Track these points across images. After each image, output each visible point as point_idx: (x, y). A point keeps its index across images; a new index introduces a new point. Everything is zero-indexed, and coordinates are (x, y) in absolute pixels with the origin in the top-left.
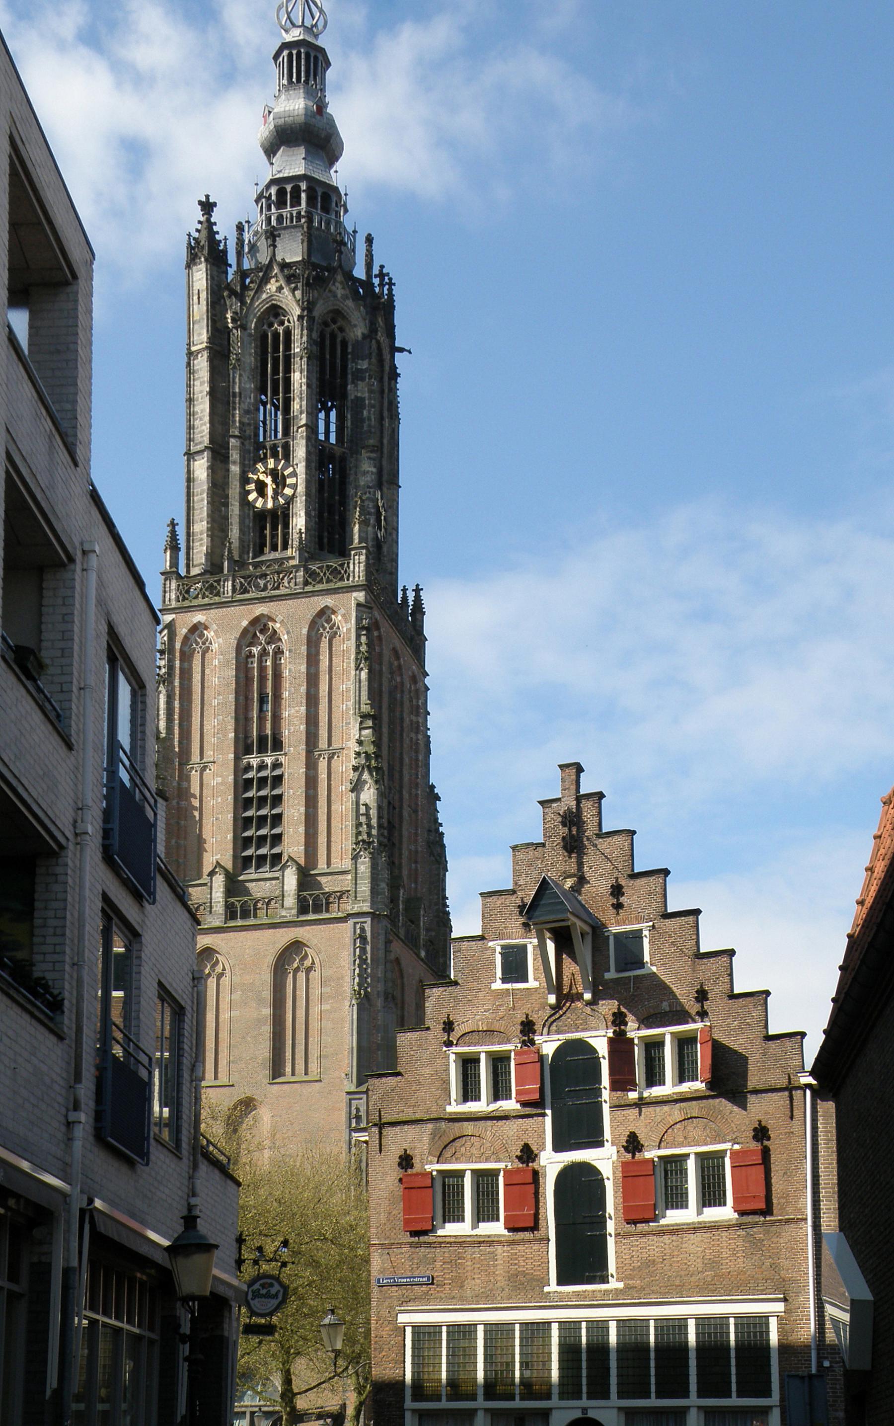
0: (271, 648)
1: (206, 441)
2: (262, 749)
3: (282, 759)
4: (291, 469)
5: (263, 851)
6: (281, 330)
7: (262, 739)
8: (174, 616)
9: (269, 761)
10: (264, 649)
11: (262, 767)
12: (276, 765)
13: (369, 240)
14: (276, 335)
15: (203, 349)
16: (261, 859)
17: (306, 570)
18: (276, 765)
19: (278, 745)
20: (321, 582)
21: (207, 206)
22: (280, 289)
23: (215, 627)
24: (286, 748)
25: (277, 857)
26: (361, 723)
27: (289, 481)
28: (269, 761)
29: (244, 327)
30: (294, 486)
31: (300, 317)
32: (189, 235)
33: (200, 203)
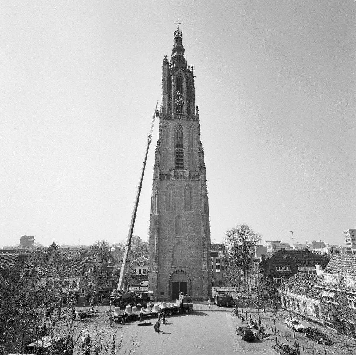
3: (183, 149)
5: (179, 166)
6: (180, 77)
7: (179, 145)
9: (181, 149)
12: (182, 150)
13: (192, 67)
14: (179, 78)
16: (180, 167)
18: (182, 150)
19: (182, 147)
21: (166, 56)
22: (180, 71)
24: (184, 146)
25: (183, 167)
27: (183, 101)
28: (181, 149)
29: (174, 75)
30: (184, 102)
31: (184, 76)
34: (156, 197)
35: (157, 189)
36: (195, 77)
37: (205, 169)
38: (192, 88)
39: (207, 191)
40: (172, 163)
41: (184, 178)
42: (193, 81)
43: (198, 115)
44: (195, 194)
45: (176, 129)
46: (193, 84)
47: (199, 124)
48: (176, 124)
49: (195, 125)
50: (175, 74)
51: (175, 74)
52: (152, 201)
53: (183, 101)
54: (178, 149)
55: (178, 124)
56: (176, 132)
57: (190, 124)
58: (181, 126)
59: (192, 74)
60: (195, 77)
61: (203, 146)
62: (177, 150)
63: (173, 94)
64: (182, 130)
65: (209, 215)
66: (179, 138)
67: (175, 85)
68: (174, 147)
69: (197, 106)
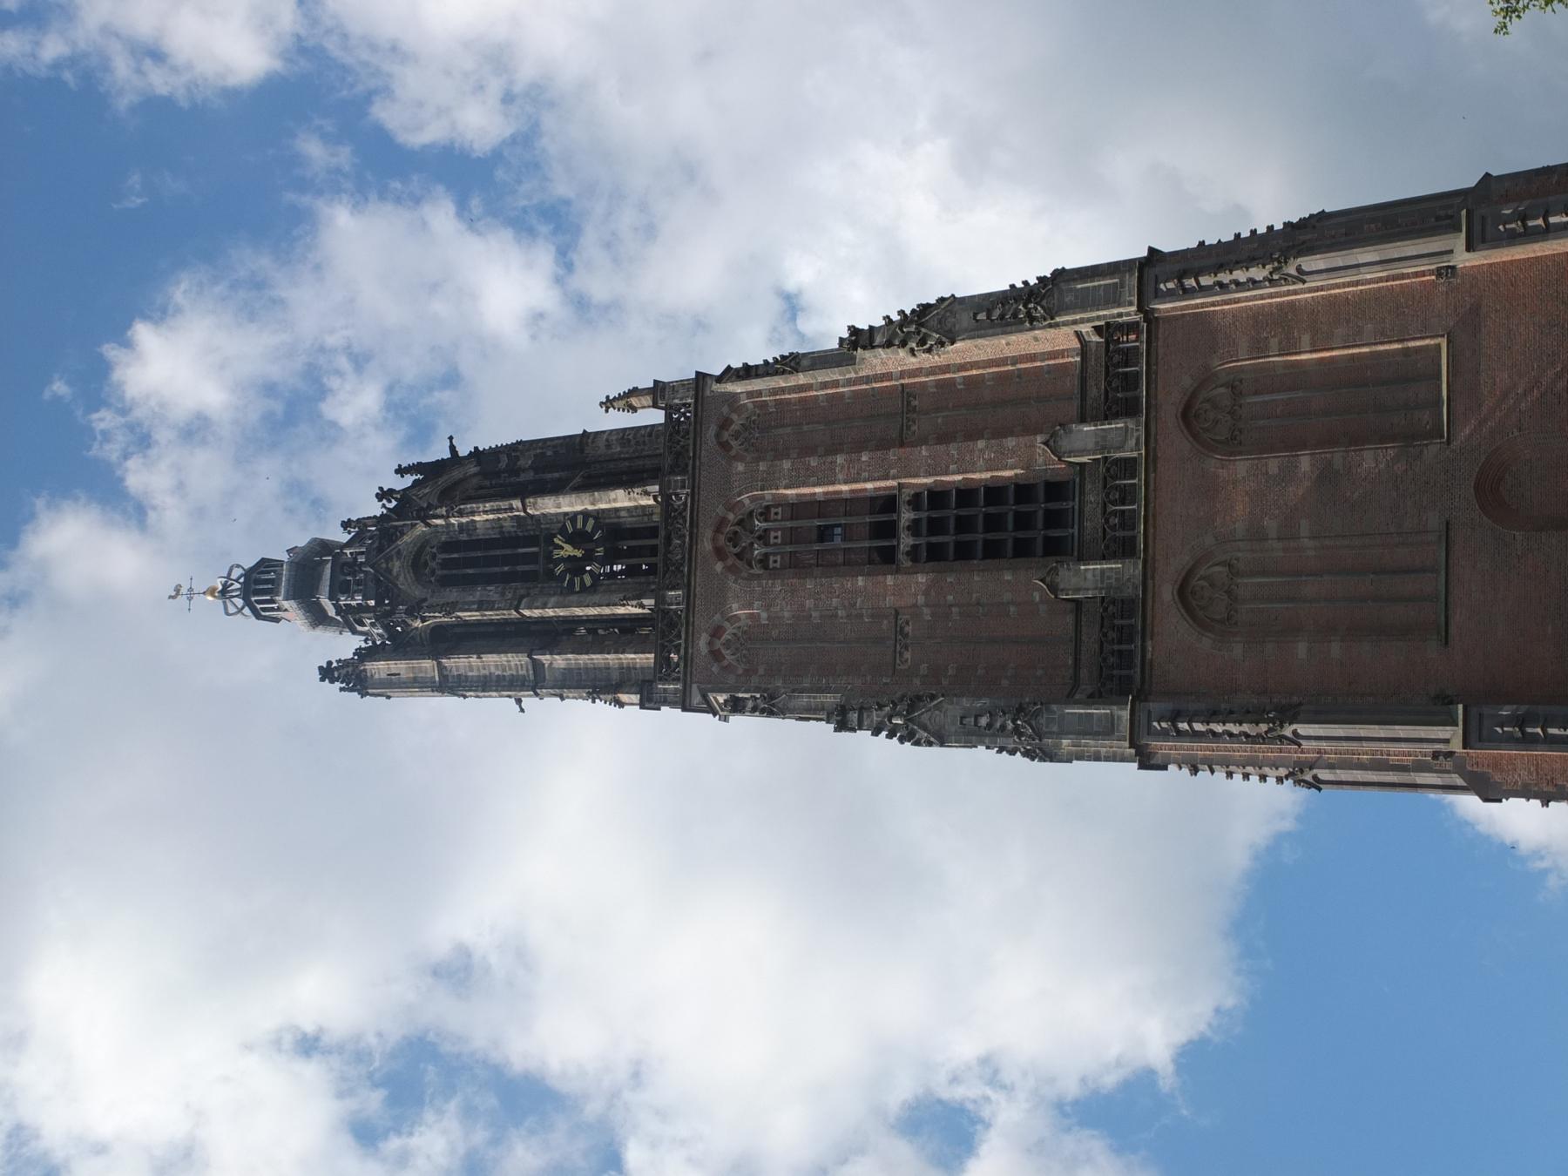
0: (759, 524)
1: (522, 659)
2: (889, 530)
3: (906, 495)
4: (568, 524)
8: (694, 686)
10: (760, 538)
11: (914, 528)
14: (445, 564)
15: (439, 664)
17: (672, 472)
20: (685, 448)
23: (717, 617)
26: (864, 348)
32: (342, 689)
33: (322, 680)
34: (1288, 731)
35: (1219, 728)
36: (452, 448)
37: (1059, 274)
38: (518, 458)
39: (1245, 234)
40: (1009, 587)
41: (1128, 466)
42: (476, 454)
43: (659, 393)
44: (1274, 342)
45: (757, 571)
46: (496, 452)
47: (717, 371)
48: (719, 567)
49: (725, 410)
50: (418, 592)
51: (418, 592)
52: (1360, 775)
53: (579, 525)
54: (906, 541)
55: (720, 553)
56: (783, 567)
57: (725, 446)
58: (740, 523)
59: (430, 471)
60: (452, 448)
61: (869, 317)
62: (913, 553)
63: (530, 607)
64: (765, 514)
65: (1470, 181)
66: (824, 534)
67: (478, 593)
68: (890, 580)
69: (608, 404)
